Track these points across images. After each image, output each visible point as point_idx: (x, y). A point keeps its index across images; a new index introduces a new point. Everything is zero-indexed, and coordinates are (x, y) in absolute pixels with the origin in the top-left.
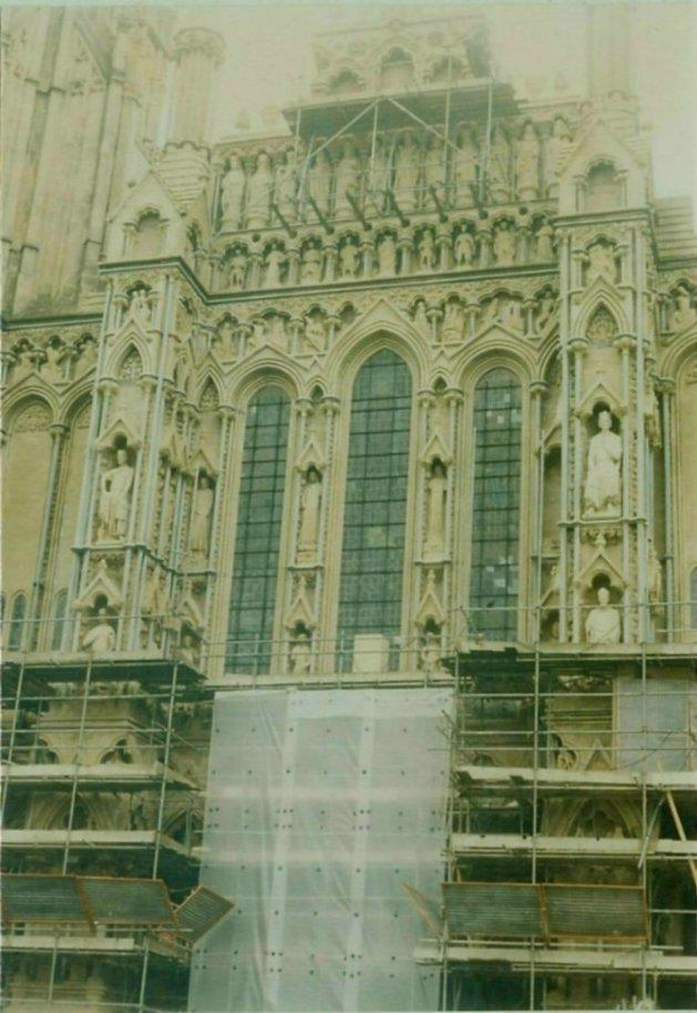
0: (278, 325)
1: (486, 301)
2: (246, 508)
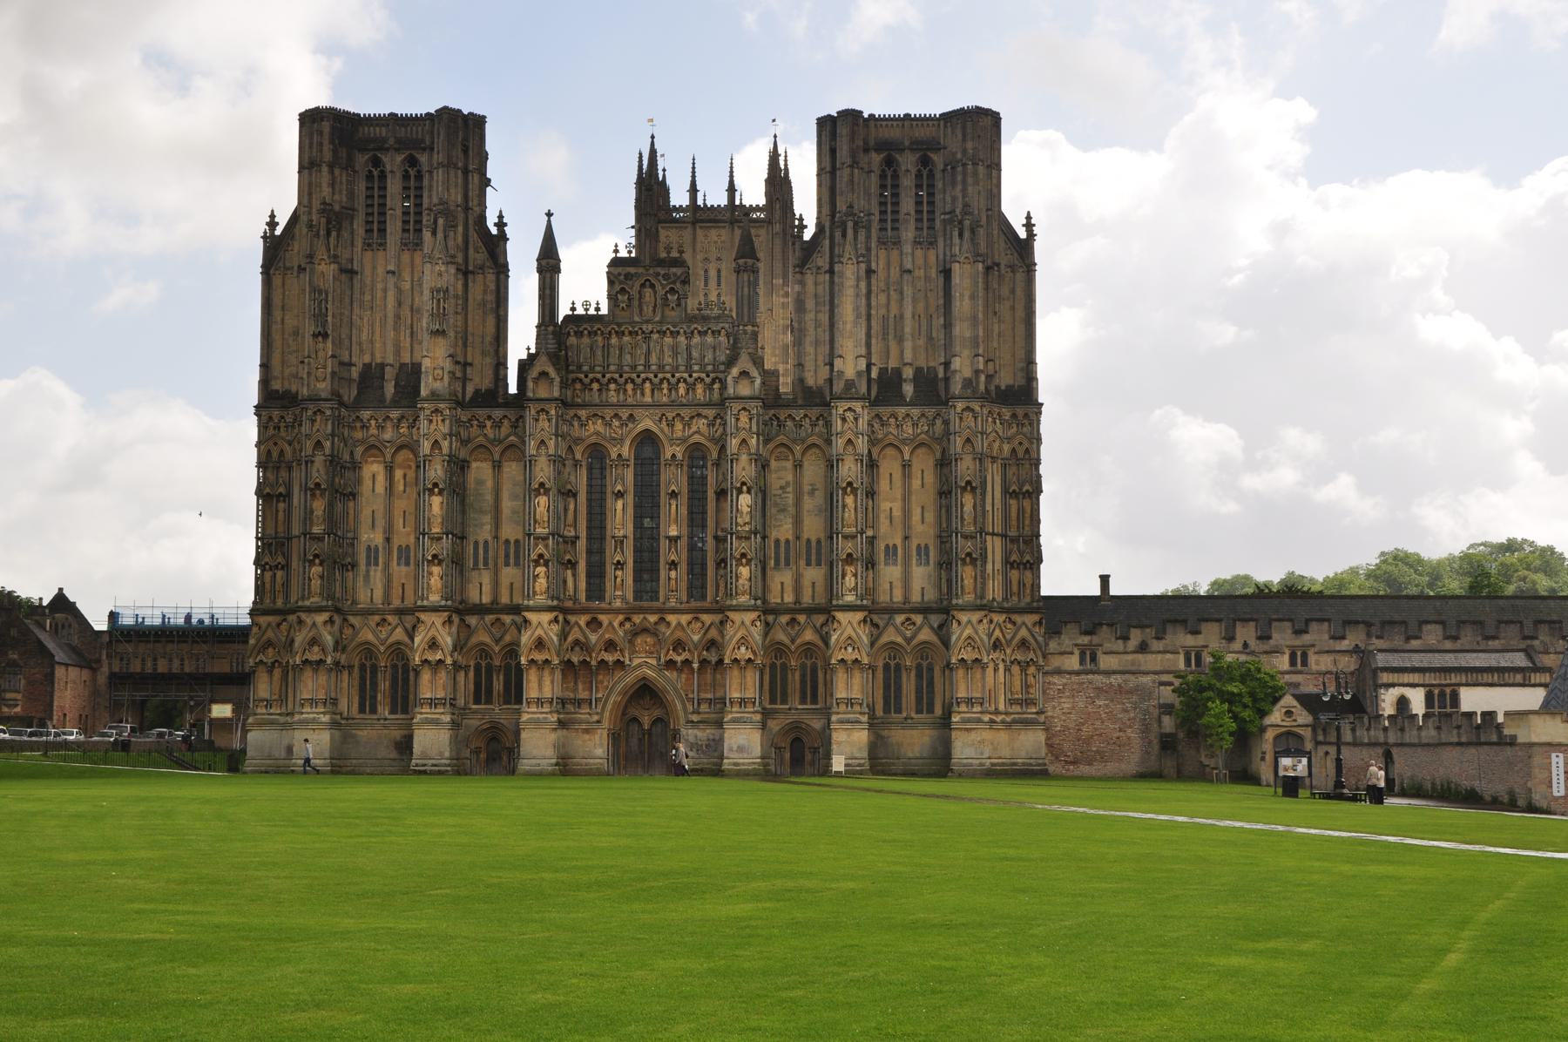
1: (692, 417)
2: (590, 507)
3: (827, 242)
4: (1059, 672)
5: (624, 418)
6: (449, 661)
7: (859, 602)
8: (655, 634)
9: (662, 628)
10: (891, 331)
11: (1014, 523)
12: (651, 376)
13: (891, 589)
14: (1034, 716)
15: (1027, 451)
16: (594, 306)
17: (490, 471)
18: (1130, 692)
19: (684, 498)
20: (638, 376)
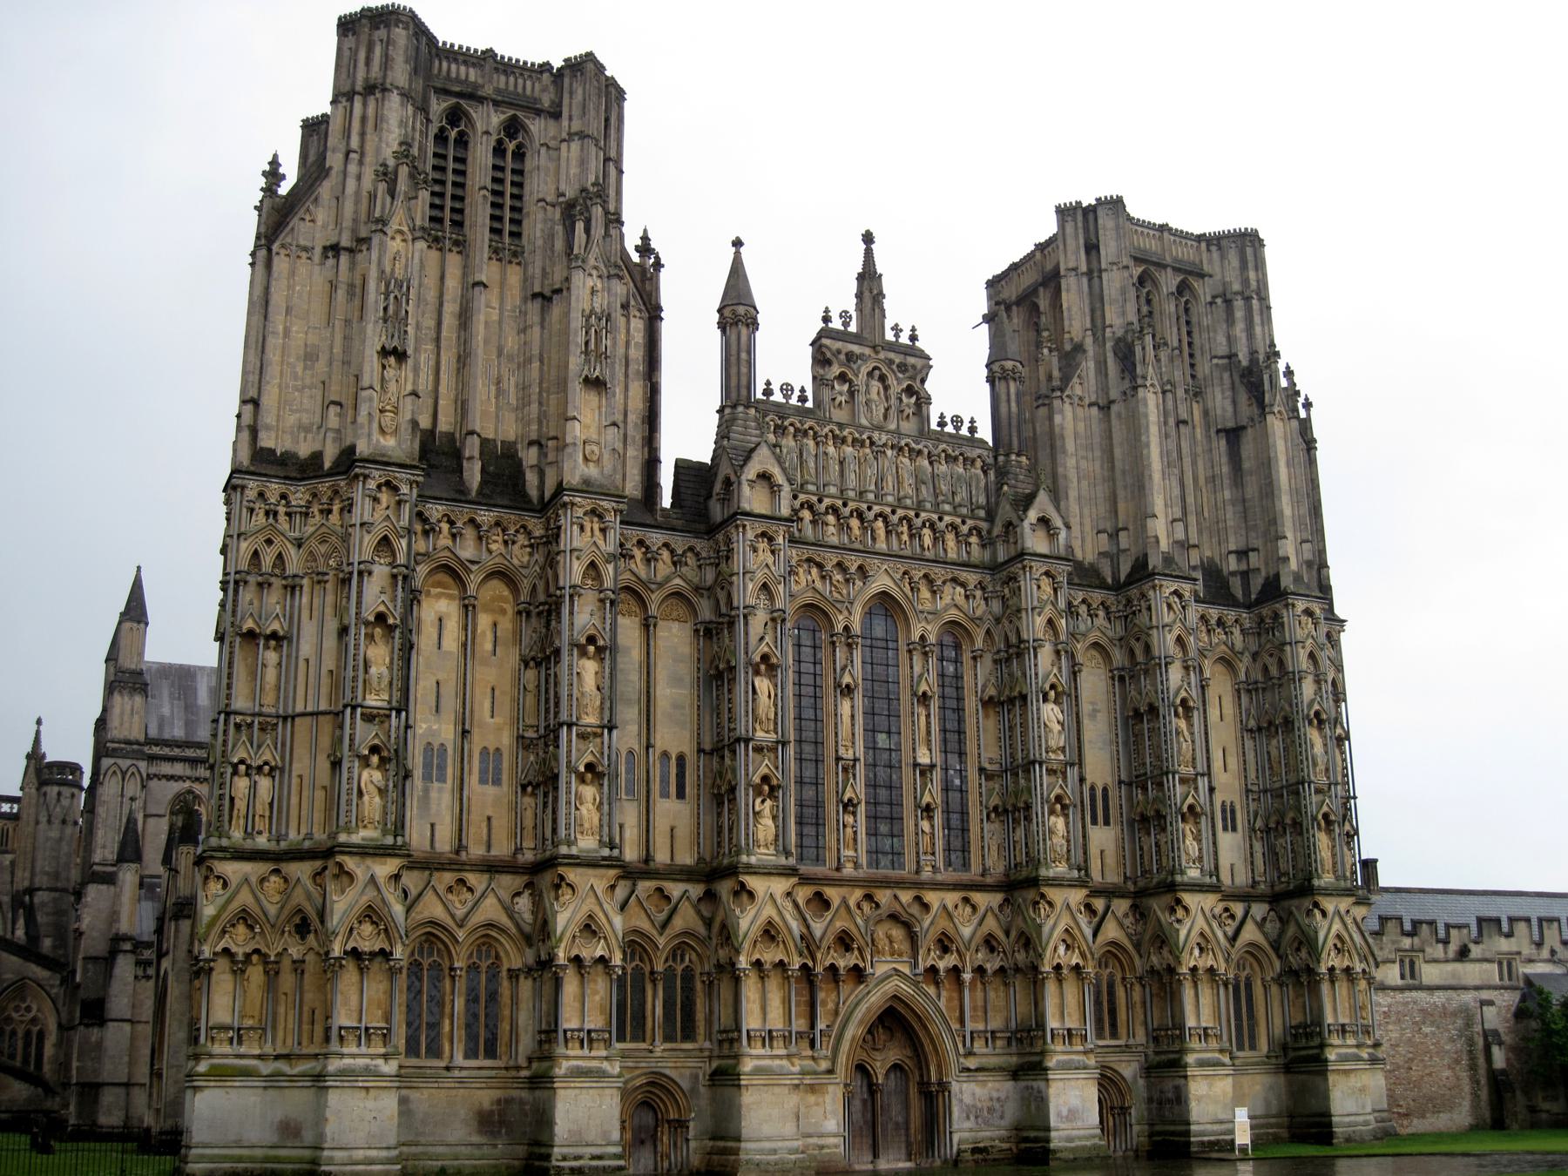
0: (814, 571)
3: (1091, 365)
4: (1383, 988)
5: (853, 569)
6: (617, 960)
9: (915, 910)
12: (888, 510)
16: (797, 393)
17: (637, 633)
18: (1454, 1014)
19: (935, 705)
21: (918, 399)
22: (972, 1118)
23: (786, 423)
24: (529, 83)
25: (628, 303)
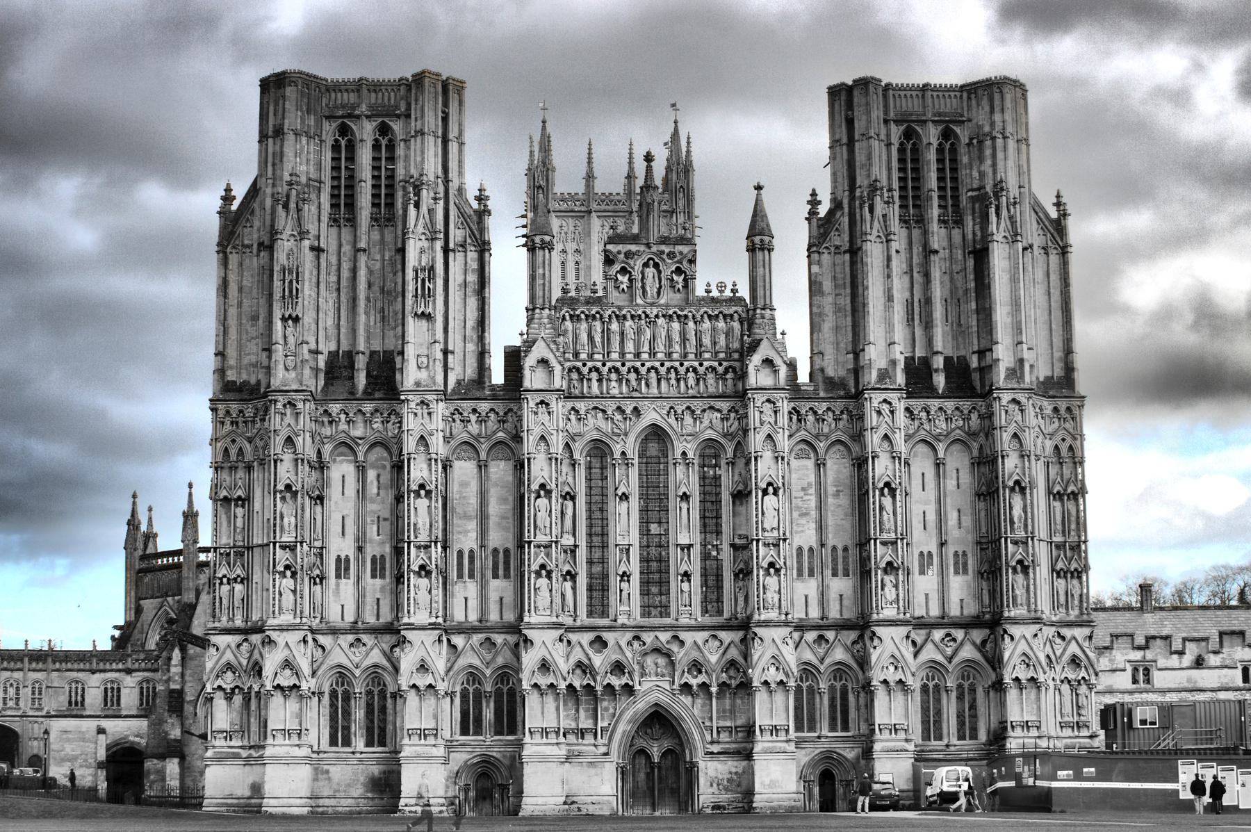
0: (600, 415)
1: (704, 411)
3: (846, 219)
5: (628, 411)
6: (442, 687)
7: (901, 616)
8: (668, 655)
9: (675, 648)
10: (917, 317)
11: (1059, 527)
13: (927, 603)
14: (1088, 740)
15: (1071, 448)
20: (643, 365)
21: (686, 276)
22: (715, 785)
23: (578, 313)
24: (392, 94)
25: (465, 241)
